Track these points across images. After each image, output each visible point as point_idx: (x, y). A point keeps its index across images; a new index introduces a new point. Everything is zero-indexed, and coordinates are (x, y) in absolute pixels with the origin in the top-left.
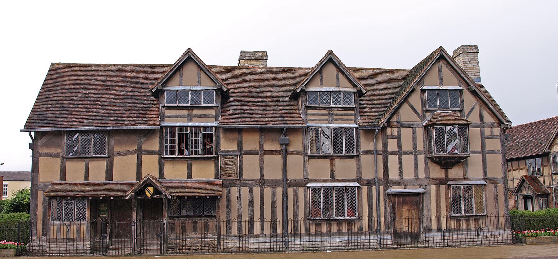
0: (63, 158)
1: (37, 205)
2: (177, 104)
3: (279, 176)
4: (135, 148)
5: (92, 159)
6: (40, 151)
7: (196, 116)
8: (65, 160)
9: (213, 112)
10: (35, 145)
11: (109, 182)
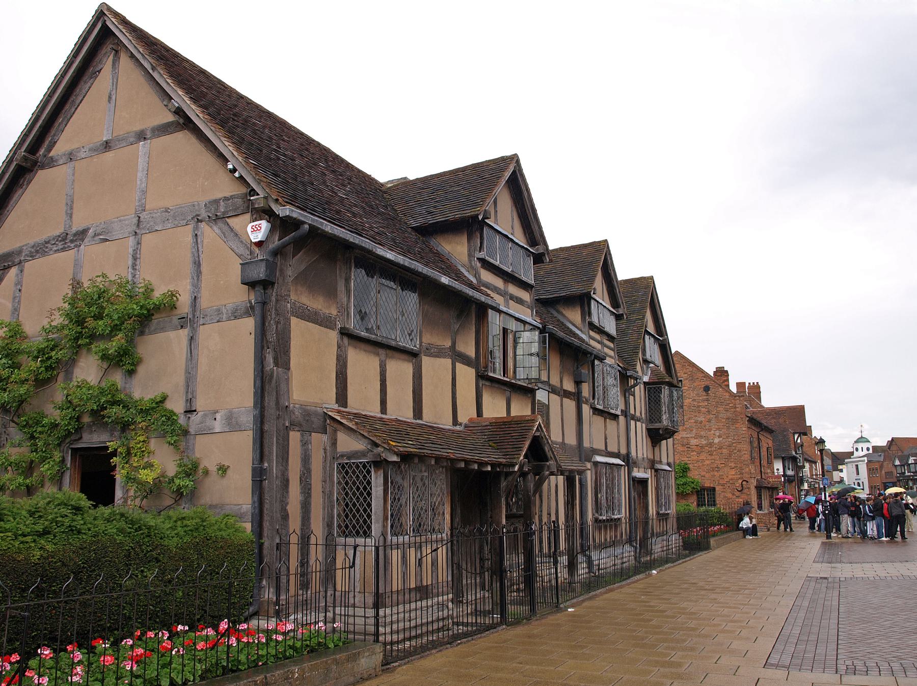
0: (345, 333)
1: (288, 481)
2: (497, 263)
3: (571, 440)
4: (448, 344)
5: (389, 352)
6: (293, 297)
7: (512, 297)
8: (346, 340)
9: (525, 296)
10: (281, 271)
11: (418, 421)
